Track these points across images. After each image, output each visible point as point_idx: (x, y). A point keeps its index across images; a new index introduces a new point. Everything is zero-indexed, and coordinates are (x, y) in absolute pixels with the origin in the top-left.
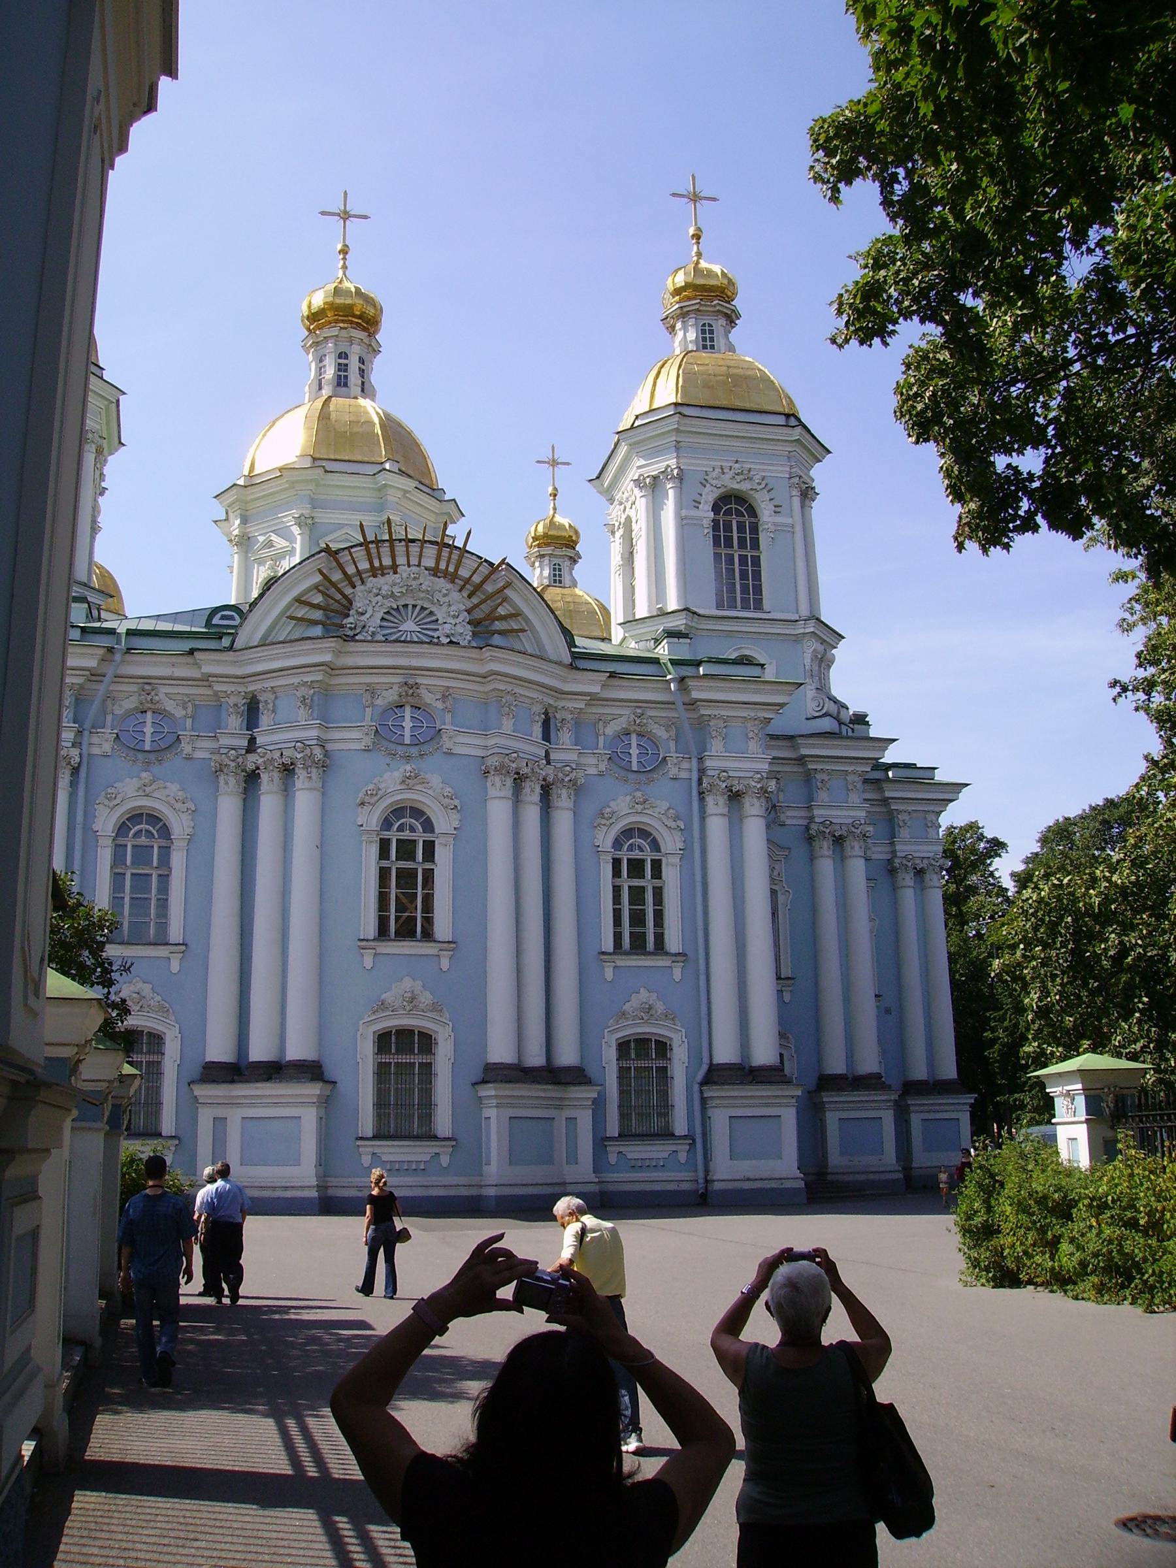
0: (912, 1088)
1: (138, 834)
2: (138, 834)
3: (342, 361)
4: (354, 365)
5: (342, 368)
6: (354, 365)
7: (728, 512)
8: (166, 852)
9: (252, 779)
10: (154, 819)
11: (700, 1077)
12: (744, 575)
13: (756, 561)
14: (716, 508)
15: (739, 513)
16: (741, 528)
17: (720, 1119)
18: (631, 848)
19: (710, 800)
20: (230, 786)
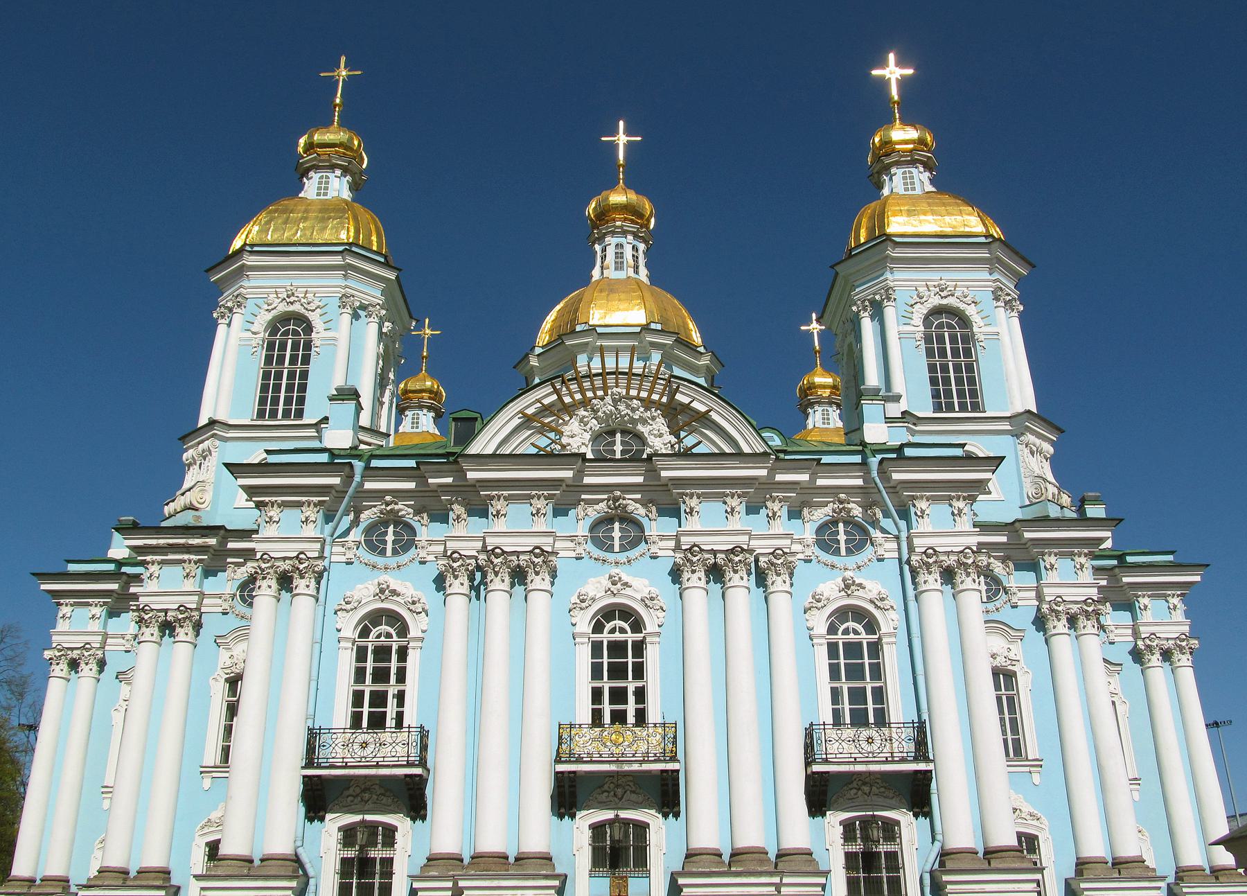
2: (379, 636)
5: (619, 255)
10: (394, 618)
12: (959, 381)
13: (970, 368)
15: (950, 326)
16: (953, 339)
18: (846, 632)
19: (921, 579)
20: (459, 585)
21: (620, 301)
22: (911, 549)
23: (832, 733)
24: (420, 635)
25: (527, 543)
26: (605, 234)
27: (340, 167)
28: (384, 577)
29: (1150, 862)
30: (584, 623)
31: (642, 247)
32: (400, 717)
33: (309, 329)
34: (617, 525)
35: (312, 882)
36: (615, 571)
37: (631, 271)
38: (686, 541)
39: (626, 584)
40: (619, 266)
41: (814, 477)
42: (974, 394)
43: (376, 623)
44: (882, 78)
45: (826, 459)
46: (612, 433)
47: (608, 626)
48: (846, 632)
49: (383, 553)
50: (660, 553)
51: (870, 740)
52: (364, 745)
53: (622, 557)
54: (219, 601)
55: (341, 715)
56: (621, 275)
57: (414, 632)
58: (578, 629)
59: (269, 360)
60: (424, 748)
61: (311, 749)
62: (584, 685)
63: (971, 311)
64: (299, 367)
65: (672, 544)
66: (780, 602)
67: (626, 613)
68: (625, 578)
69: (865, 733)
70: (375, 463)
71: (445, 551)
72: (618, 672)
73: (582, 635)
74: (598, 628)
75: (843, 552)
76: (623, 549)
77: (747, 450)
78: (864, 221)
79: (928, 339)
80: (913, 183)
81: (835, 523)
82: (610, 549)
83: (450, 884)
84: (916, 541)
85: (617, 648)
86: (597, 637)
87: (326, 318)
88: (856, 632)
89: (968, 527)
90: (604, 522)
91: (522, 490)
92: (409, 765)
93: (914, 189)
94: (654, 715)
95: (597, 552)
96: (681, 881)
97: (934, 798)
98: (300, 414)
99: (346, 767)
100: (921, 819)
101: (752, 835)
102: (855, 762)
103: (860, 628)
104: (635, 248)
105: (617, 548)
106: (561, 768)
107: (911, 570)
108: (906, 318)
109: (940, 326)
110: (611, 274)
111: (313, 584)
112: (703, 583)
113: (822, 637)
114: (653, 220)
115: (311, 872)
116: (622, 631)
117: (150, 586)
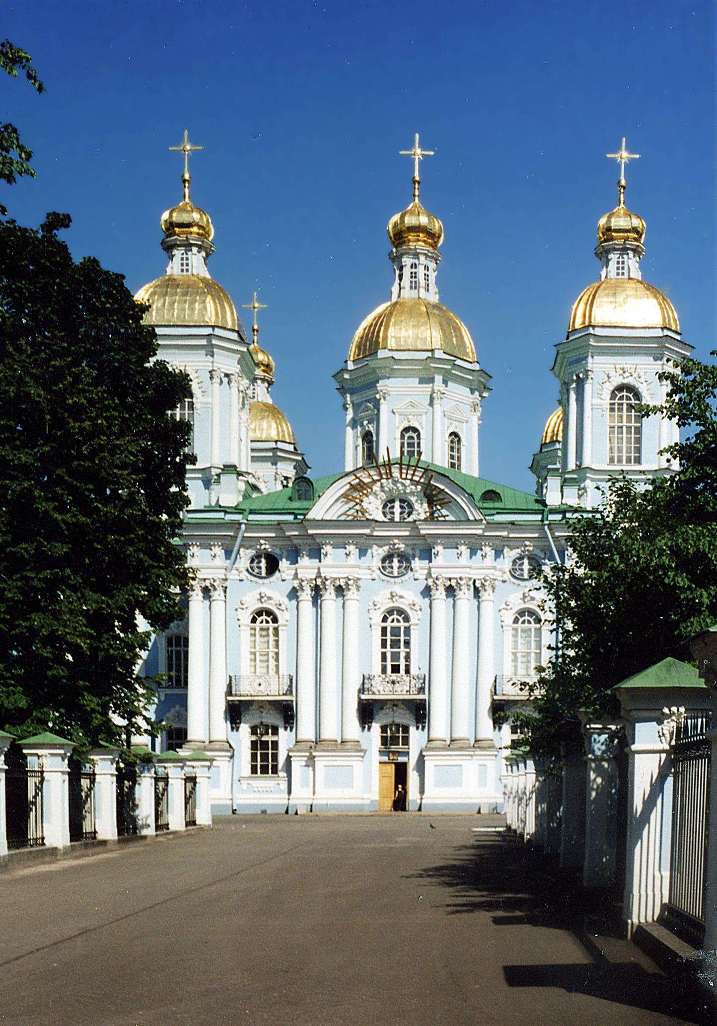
1: (262, 622)
2: (262, 622)
3: (414, 270)
5: (414, 275)
7: (621, 398)
9: (317, 593)
14: (613, 396)
15: (628, 398)
21: (413, 321)
24: (285, 623)
26: (402, 255)
27: (196, 245)
30: (377, 617)
31: (432, 265)
34: (395, 560)
37: (422, 291)
39: (401, 597)
40: (415, 286)
41: (509, 533)
44: (614, 160)
46: (392, 501)
47: (390, 619)
48: (523, 622)
50: (420, 577)
58: (372, 622)
60: (291, 686)
61: (230, 686)
62: (377, 650)
65: (426, 571)
66: (488, 608)
67: (401, 612)
70: (251, 517)
71: (296, 574)
72: (395, 644)
74: (385, 619)
77: (471, 518)
78: (586, 297)
80: (623, 268)
81: (521, 558)
83: (308, 754)
85: (396, 631)
86: (384, 624)
90: (388, 558)
91: (340, 542)
93: (623, 274)
94: (414, 671)
96: (424, 753)
101: (463, 731)
104: (427, 268)
109: (621, 398)
110: (408, 294)
111: (223, 594)
114: (442, 238)
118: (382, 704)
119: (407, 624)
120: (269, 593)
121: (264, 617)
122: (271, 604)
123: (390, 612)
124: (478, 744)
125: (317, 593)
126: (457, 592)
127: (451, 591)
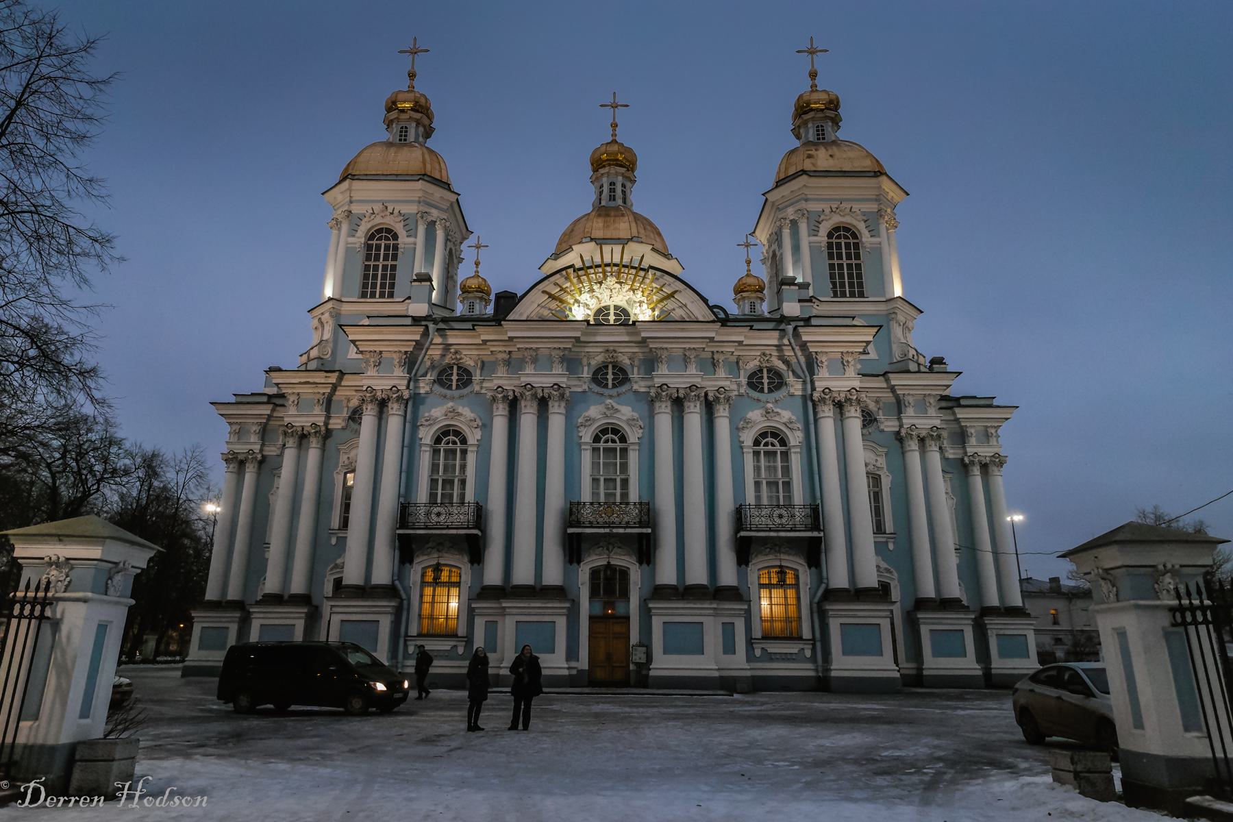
0: (987, 611)
4: (619, 189)
5: (612, 190)
6: (619, 189)
7: (839, 237)
8: (464, 452)
9: (513, 405)
11: (816, 600)
12: (850, 276)
13: (859, 266)
14: (830, 235)
15: (846, 237)
16: (848, 245)
17: (834, 625)
18: (766, 444)
19: (819, 409)
20: (501, 411)
22: (813, 389)
23: (755, 512)
25: (547, 381)
28: (450, 404)
29: (965, 602)
32: (462, 496)
33: (396, 237)
35: (405, 602)
36: (609, 401)
38: (658, 381)
42: (861, 285)
43: (446, 433)
45: (756, 326)
49: (450, 387)
51: (781, 516)
52: (439, 514)
53: (614, 392)
54: (339, 421)
55: (422, 495)
56: (612, 204)
57: (472, 440)
59: (368, 258)
63: (861, 226)
64: (390, 263)
66: (723, 426)
68: (616, 406)
69: (777, 512)
73: (586, 443)
74: (597, 439)
75: (766, 390)
76: (614, 386)
79: (830, 246)
82: (606, 386)
84: (817, 384)
86: (596, 445)
87: (408, 228)
88: (773, 445)
89: (853, 375)
92: (468, 528)
94: (634, 496)
95: (596, 388)
97: (823, 555)
98: (391, 295)
99: (426, 528)
100: (813, 569)
102: (770, 530)
103: (776, 442)
105: (610, 385)
106: (570, 531)
107: (810, 404)
108: (814, 232)
111: (403, 407)
112: (669, 410)
113: (749, 447)
115: (404, 596)
116: (614, 441)
117: (292, 410)
118: (596, 540)
119: (623, 445)
120: (460, 410)
121: (451, 437)
122: (461, 422)
123: (604, 431)
124: (715, 593)
125: (513, 405)
126: (686, 404)
127: (678, 403)
